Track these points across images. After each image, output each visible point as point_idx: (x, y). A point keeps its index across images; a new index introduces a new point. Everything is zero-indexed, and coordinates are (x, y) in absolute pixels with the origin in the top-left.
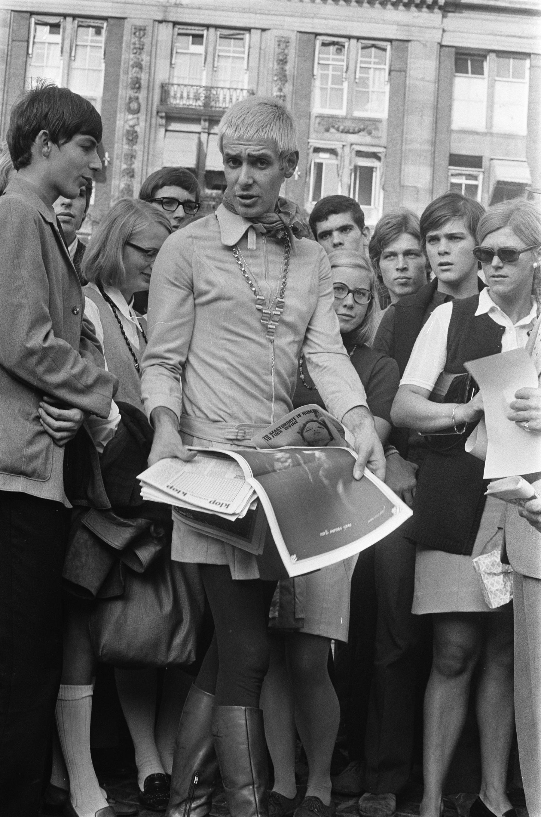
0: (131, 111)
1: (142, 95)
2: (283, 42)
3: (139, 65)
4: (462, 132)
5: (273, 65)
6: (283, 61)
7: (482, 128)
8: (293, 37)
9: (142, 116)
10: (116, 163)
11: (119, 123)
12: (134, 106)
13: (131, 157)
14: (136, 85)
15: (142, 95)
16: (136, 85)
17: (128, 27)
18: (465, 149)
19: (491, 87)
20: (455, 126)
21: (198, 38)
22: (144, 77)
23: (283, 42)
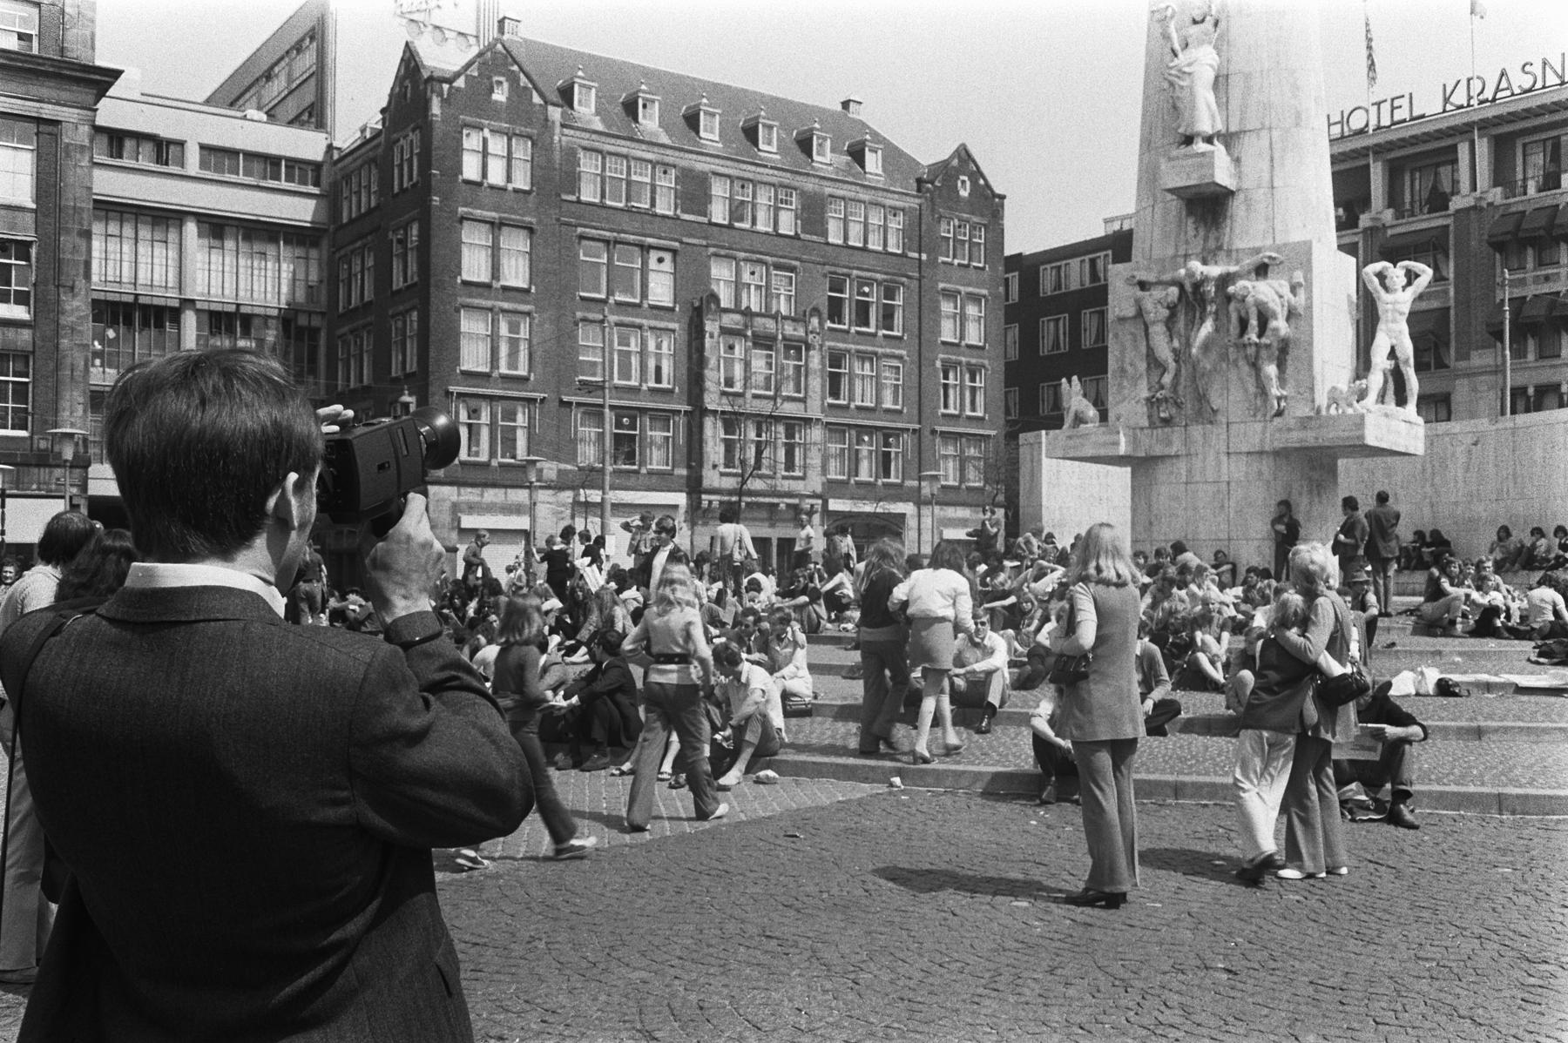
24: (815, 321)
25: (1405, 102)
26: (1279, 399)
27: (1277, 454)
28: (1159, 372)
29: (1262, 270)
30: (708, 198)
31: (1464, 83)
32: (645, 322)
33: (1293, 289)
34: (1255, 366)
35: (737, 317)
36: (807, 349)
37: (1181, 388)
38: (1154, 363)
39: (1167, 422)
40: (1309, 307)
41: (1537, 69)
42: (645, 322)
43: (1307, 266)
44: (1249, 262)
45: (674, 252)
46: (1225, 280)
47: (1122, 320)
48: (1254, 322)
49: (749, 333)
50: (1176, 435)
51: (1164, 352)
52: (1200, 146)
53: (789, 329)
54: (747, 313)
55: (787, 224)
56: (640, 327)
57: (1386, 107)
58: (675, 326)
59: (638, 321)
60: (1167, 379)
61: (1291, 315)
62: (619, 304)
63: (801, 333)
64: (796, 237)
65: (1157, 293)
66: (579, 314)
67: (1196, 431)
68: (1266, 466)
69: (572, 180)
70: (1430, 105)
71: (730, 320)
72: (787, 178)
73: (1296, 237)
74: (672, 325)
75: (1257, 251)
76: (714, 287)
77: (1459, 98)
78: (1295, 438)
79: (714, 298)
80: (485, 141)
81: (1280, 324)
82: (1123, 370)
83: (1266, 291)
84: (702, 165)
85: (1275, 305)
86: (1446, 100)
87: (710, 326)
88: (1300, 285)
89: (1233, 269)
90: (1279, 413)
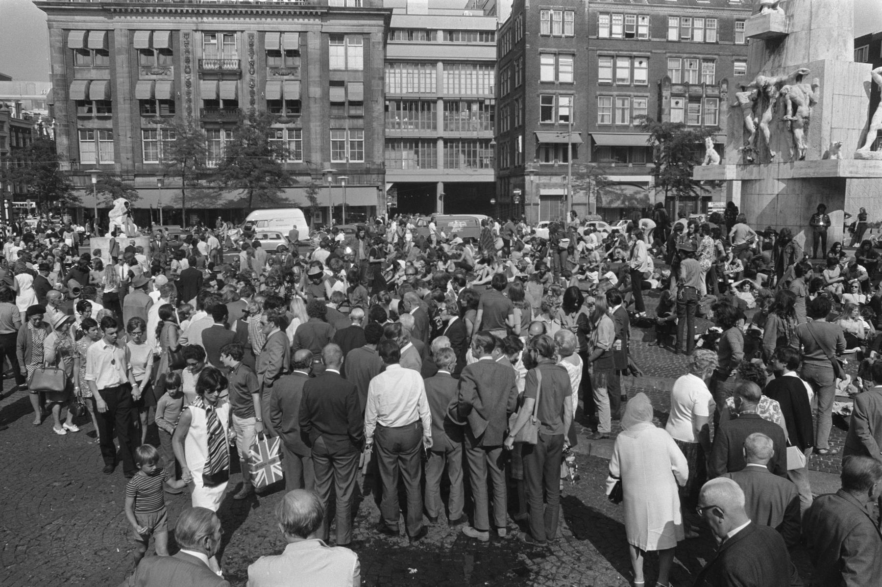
0: (186, 73)
1: (191, 65)
2: (251, 36)
3: (187, 51)
4: (335, 71)
5: (248, 47)
6: (251, 45)
7: (343, 68)
8: (256, 33)
9: (192, 75)
10: (183, 96)
11: (183, 78)
12: (188, 70)
13: (189, 93)
14: (188, 60)
15: (191, 65)
16: (188, 60)
17: (181, 33)
18: (337, 78)
19: (346, 50)
20: (331, 68)
21: (214, 37)
22: (191, 56)
23: (251, 36)
24: (725, 86)
26: (803, 150)
27: (804, 180)
28: (747, 135)
29: (799, 78)
30: (666, 28)
32: (632, 94)
33: (814, 87)
34: (792, 131)
35: (680, 87)
36: (720, 101)
37: (758, 143)
39: (751, 162)
40: (821, 98)
42: (632, 94)
43: (821, 76)
44: (792, 73)
46: (780, 85)
48: (790, 108)
49: (687, 95)
52: (766, 11)
53: (710, 91)
54: (686, 85)
55: (712, 37)
56: (630, 96)
58: (648, 94)
59: (628, 93)
60: (751, 139)
61: (812, 103)
62: (619, 86)
63: (716, 92)
64: (717, 43)
65: (748, 93)
66: (598, 93)
68: (798, 185)
69: (595, 28)
71: (675, 89)
72: (711, 13)
73: (821, 58)
74: (645, 94)
75: (798, 67)
76: (669, 74)
78: (811, 173)
79: (668, 79)
80: (551, 16)
81: (804, 109)
83: (795, 91)
84: (662, 11)
85: (800, 98)
87: (666, 93)
88: (816, 86)
89: (785, 78)
90: (803, 158)
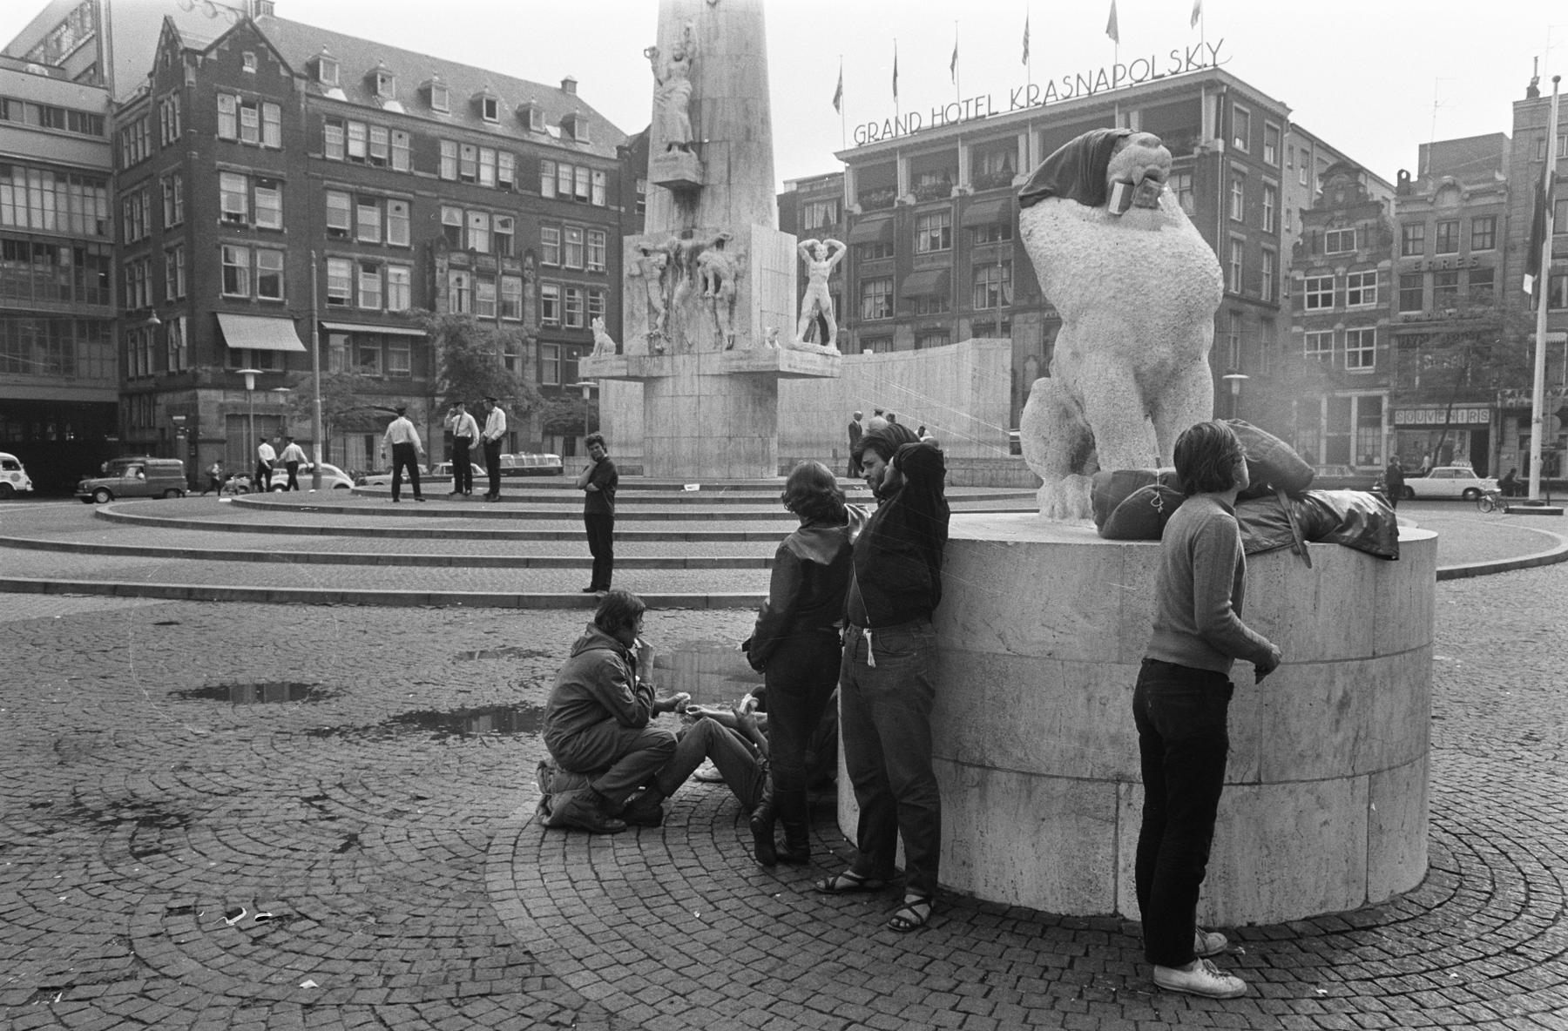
25: (984, 101)
27: (731, 375)
31: (1024, 91)
38: (653, 310)
41: (1073, 81)
45: (410, 202)
47: (632, 277)
50: (666, 361)
51: (658, 304)
57: (972, 105)
60: (660, 321)
63: (518, 269)
67: (679, 359)
68: (725, 384)
70: (1002, 107)
77: (1022, 100)
82: (632, 314)
86: (1013, 101)
